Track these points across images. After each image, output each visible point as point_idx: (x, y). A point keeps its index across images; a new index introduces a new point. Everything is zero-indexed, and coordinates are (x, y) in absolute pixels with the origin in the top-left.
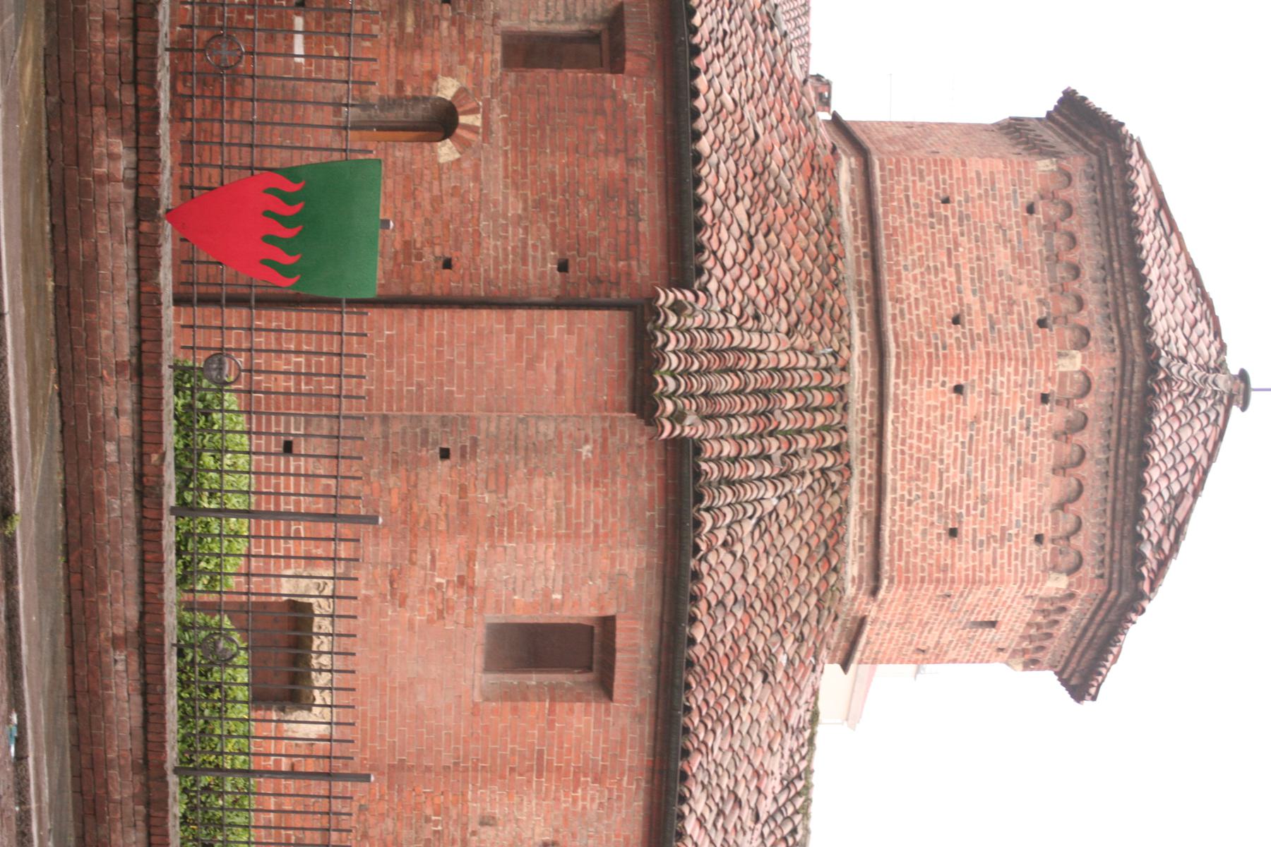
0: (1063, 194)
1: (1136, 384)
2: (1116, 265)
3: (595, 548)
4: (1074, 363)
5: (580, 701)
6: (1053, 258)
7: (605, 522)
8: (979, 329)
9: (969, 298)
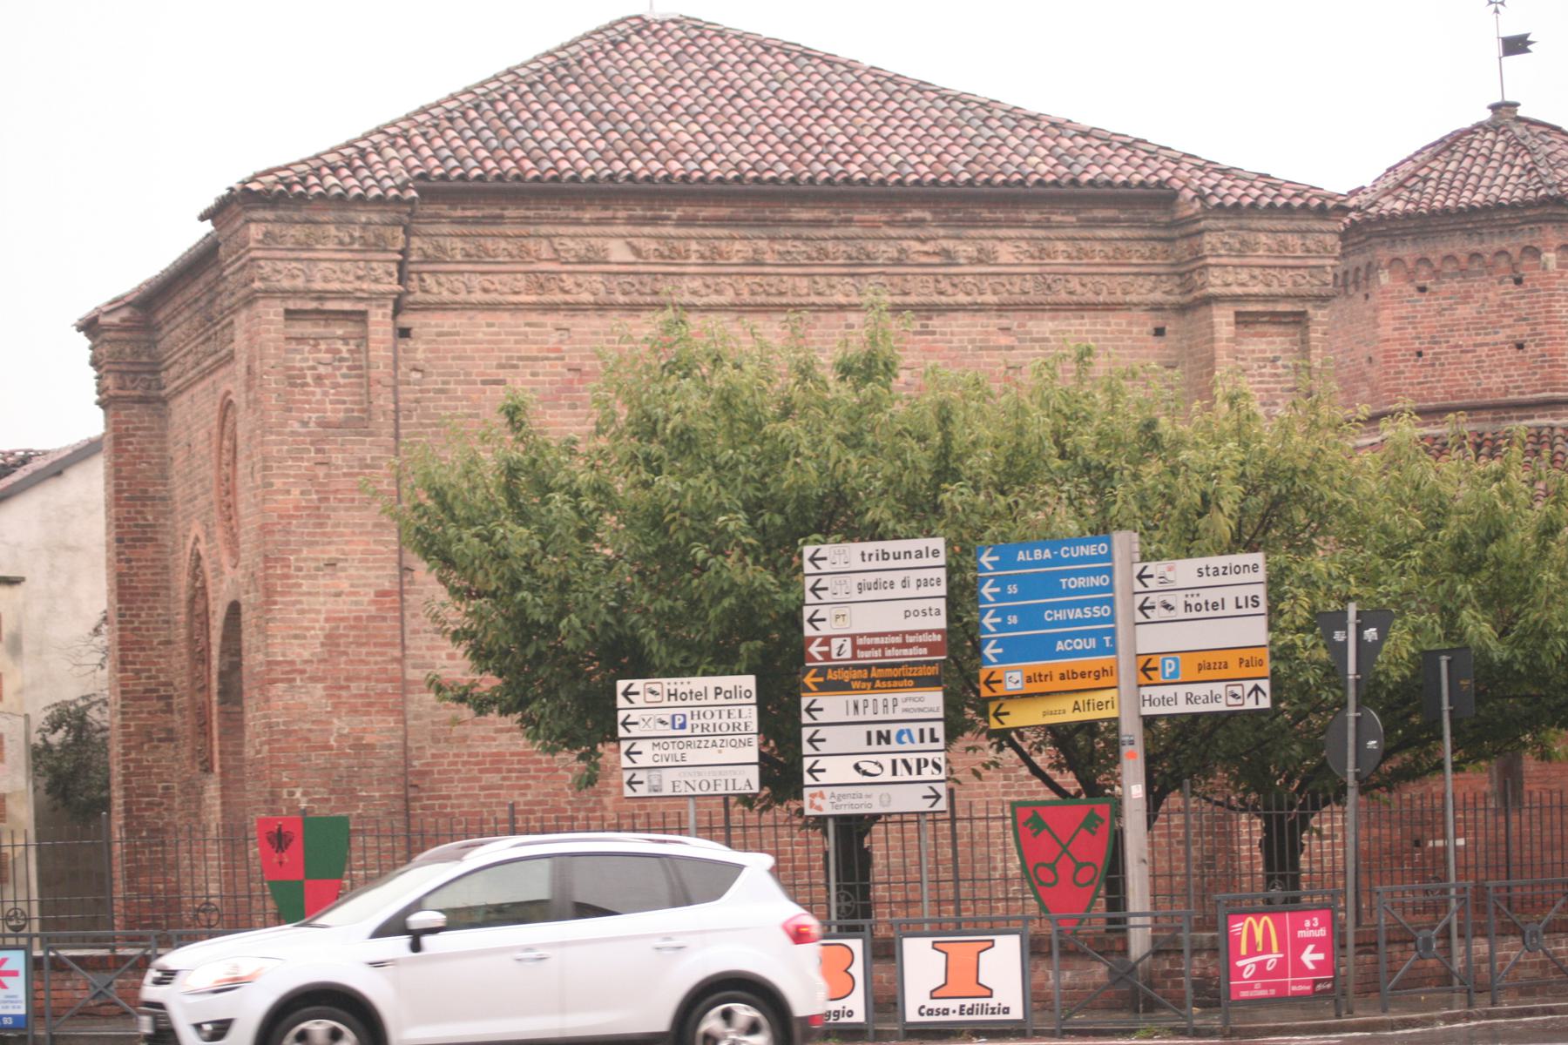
0: (1410, 265)
4: (1551, 258)
6: (1464, 273)
8: (1527, 330)
9: (1501, 336)
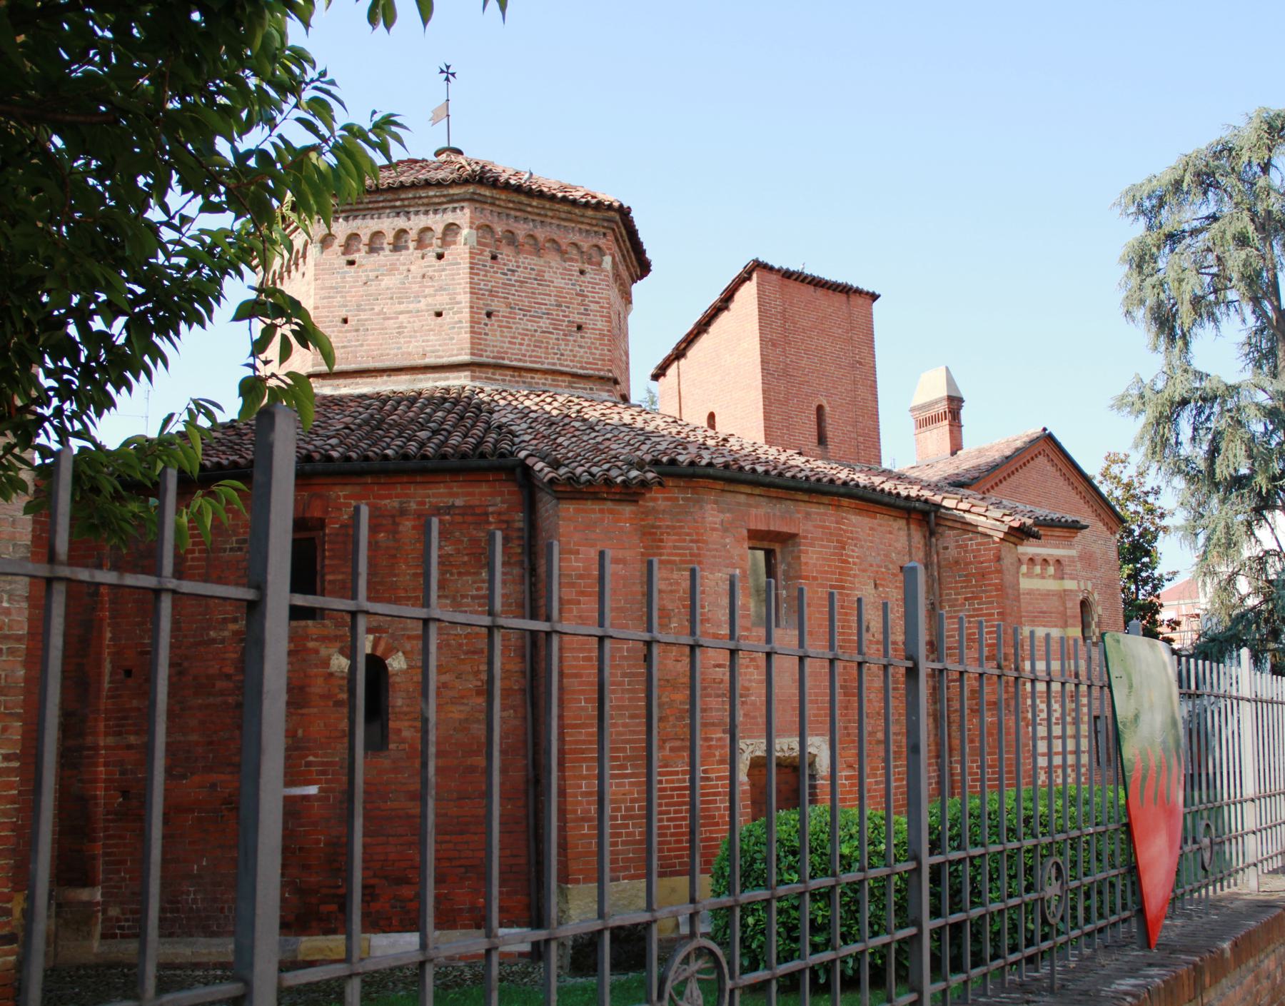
1: (488, 193)
2: (398, 203)
3: (705, 542)
5: (799, 557)
7: (688, 534)
9: (422, 305)
